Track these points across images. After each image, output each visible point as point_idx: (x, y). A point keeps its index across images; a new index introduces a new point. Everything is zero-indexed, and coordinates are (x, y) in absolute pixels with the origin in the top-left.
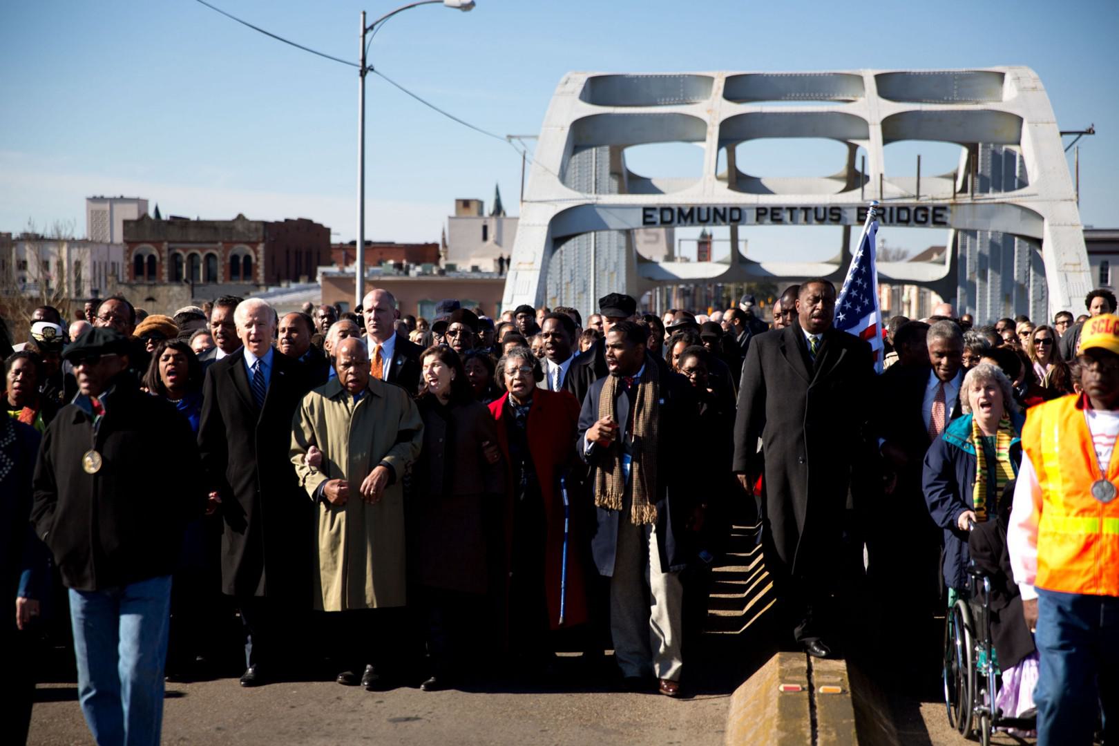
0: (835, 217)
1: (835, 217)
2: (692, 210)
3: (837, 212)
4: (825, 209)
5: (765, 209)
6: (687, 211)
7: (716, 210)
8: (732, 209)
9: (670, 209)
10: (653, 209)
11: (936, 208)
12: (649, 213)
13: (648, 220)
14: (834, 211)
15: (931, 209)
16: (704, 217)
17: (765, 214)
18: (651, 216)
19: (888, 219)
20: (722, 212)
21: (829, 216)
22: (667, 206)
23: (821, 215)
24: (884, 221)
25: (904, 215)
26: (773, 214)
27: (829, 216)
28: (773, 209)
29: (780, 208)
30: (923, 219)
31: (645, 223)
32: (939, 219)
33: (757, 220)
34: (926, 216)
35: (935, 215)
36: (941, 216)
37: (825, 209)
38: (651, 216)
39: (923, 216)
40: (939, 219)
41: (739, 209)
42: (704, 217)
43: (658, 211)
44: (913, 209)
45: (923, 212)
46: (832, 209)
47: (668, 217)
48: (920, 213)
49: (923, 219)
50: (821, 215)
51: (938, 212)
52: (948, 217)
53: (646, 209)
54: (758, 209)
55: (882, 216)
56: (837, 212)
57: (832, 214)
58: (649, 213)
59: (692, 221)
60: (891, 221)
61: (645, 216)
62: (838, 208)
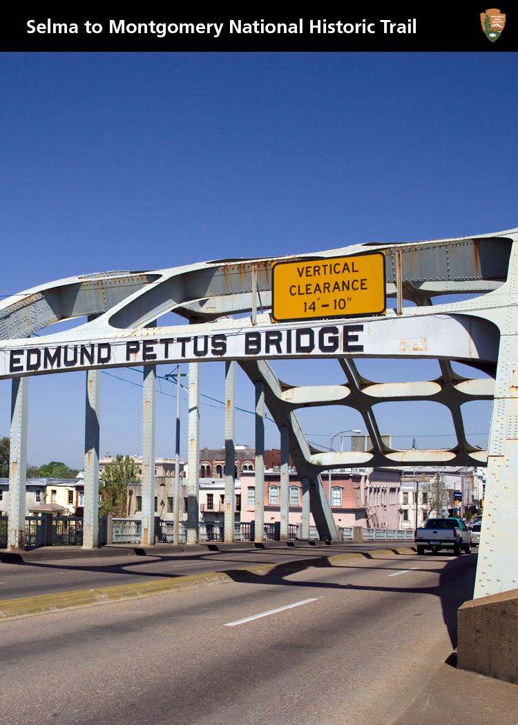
2: (59, 349)
3: (221, 341)
5: (136, 343)
6: (52, 353)
7: (83, 349)
8: (101, 346)
9: (37, 351)
10: (20, 352)
12: (15, 357)
13: (15, 365)
15: (341, 329)
16: (71, 357)
17: (136, 351)
18: (18, 361)
19: (283, 344)
20: (89, 350)
21: (210, 347)
22: (34, 347)
23: (201, 348)
24: (279, 350)
26: (145, 349)
27: (210, 347)
28: (145, 342)
30: (332, 344)
31: (12, 369)
32: (351, 344)
33: (128, 358)
34: (334, 340)
35: (347, 338)
36: (355, 338)
37: (206, 337)
38: (18, 361)
39: (331, 339)
40: (351, 344)
41: (107, 346)
42: (70, 358)
43: (26, 352)
45: (331, 335)
48: (326, 336)
49: (332, 344)
50: (201, 348)
53: (13, 352)
54: (129, 343)
55: (277, 343)
56: (221, 341)
57: (214, 344)
58: (15, 357)
59: (59, 365)
60: (289, 350)
61: (13, 361)
62: (223, 337)
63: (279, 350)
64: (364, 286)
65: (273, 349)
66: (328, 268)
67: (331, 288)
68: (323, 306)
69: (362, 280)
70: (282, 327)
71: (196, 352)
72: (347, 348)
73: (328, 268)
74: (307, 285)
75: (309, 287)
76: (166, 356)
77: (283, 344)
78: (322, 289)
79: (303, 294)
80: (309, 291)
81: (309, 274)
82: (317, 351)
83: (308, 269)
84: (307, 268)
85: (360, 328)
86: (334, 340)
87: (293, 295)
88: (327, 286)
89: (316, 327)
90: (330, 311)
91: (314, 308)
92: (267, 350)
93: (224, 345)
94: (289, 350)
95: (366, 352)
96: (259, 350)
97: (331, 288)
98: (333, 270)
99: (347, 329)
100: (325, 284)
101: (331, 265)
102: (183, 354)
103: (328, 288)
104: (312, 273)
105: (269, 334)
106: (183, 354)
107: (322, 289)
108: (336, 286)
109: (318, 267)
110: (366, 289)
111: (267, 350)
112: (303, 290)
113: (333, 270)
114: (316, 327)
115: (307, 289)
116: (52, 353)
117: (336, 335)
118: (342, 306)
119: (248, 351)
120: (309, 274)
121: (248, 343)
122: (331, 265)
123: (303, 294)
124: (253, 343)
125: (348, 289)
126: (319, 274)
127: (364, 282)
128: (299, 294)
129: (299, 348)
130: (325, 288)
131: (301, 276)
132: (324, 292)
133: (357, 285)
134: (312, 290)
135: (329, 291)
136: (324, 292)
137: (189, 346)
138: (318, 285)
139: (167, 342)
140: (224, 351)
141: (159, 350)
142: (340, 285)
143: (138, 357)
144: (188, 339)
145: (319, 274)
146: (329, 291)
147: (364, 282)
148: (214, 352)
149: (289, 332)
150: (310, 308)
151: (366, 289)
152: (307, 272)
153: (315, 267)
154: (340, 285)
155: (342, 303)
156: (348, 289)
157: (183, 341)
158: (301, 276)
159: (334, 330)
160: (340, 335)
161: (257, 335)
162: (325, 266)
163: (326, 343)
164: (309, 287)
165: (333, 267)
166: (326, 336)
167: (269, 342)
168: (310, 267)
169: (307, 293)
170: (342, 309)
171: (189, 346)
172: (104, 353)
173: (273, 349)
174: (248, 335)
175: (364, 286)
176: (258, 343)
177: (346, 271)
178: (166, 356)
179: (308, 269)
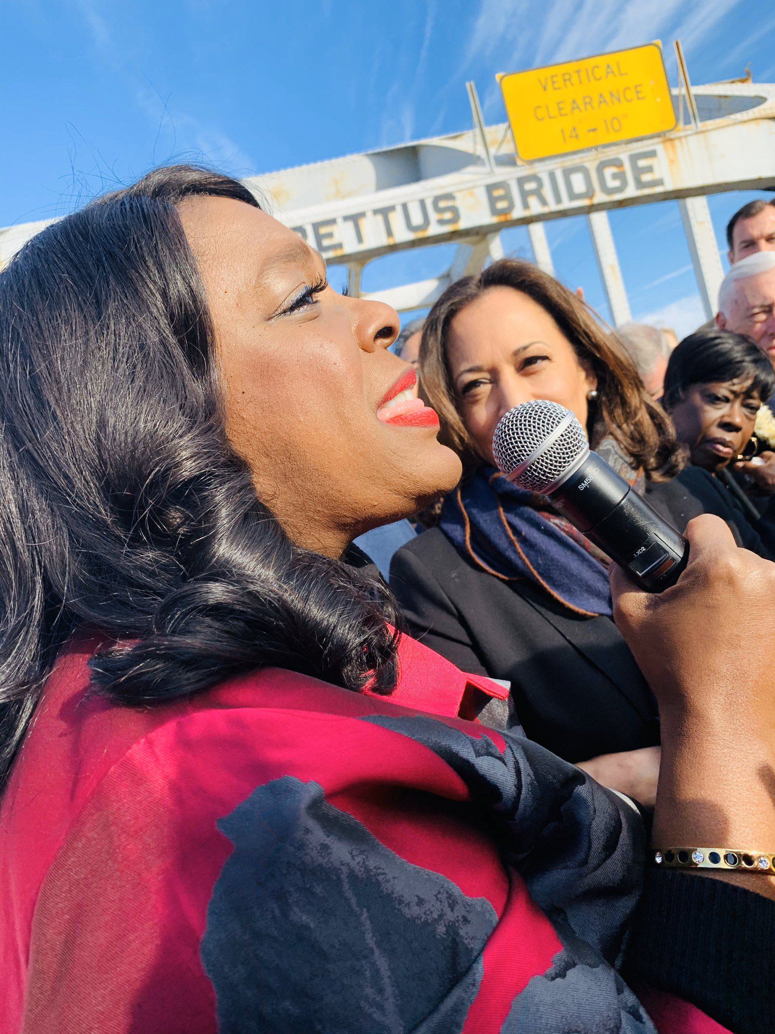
0: (448, 216)
1: (448, 216)
3: (449, 203)
4: (422, 203)
11: (634, 158)
14: (442, 204)
15: (625, 158)
19: (547, 192)
21: (433, 216)
23: (417, 219)
24: (544, 202)
29: (332, 222)
30: (616, 183)
32: (646, 178)
34: (620, 176)
35: (638, 172)
36: (650, 169)
39: (615, 176)
40: (646, 178)
44: (592, 167)
46: (437, 199)
48: (609, 172)
49: (616, 183)
50: (417, 219)
51: (642, 163)
55: (538, 193)
56: (449, 203)
60: (558, 200)
62: (449, 197)
63: (544, 202)
64: (640, 95)
65: (533, 201)
66: (583, 74)
67: (595, 103)
68: (589, 131)
69: (636, 87)
70: (542, 170)
71: (410, 227)
72: (640, 184)
73: (583, 74)
74: (558, 104)
75: (561, 105)
76: (360, 239)
77: (547, 192)
78: (582, 107)
79: (555, 117)
80: (563, 112)
81: (556, 86)
83: (555, 79)
84: (552, 77)
85: (652, 154)
86: (620, 176)
87: (539, 120)
88: (588, 100)
89: (591, 162)
90: (604, 137)
91: (577, 136)
92: (526, 206)
93: (454, 210)
94: (558, 200)
95: (669, 186)
96: (511, 207)
97: (595, 103)
98: (592, 78)
99: (634, 158)
100: (584, 98)
101: (587, 70)
102: (390, 233)
103: (590, 103)
104: (560, 83)
105: (521, 181)
106: (390, 233)
107: (582, 107)
108: (602, 100)
109: (567, 74)
110: (643, 98)
111: (526, 206)
112: (554, 111)
113: (592, 78)
114: (591, 162)
115: (560, 109)
117: (621, 169)
118: (616, 126)
119: (494, 211)
120: (556, 86)
121: (492, 201)
122: (587, 70)
123: (555, 117)
124: (501, 198)
125: (619, 100)
126: (572, 84)
127: (639, 89)
128: (551, 117)
129: (573, 196)
130: (586, 104)
131: (545, 89)
132: (586, 109)
133: (631, 94)
134: (567, 108)
135: (593, 108)
136: (586, 109)
137: (397, 219)
138: (574, 102)
139: (355, 219)
140: (455, 219)
142: (608, 98)
144: (392, 208)
145: (572, 84)
146: (593, 108)
147: (639, 89)
148: (441, 222)
150: (571, 137)
151: (643, 98)
152: (553, 83)
153: (564, 75)
154: (608, 98)
155: (615, 121)
156: (619, 100)
157: (384, 212)
158: (545, 89)
159: (617, 163)
162: (578, 72)
164: (561, 105)
165: (590, 74)
166: (609, 172)
167: (525, 195)
168: (556, 76)
169: (562, 115)
170: (616, 131)
171: (397, 219)
173: (533, 201)
174: (490, 188)
175: (640, 95)
176: (507, 197)
177: (610, 75)
178: (360, 239)
179: (555, 79)
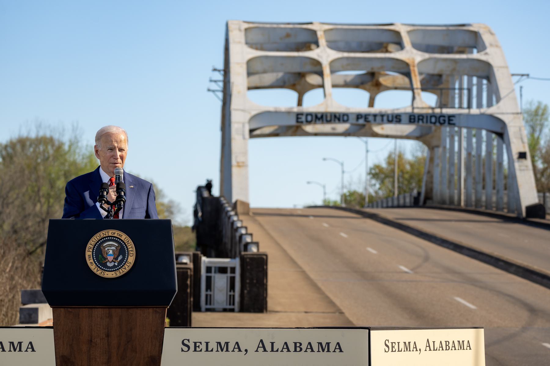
6: (319, 116)
16: (329, 119)
19: (425, 120)
21: (395, 119)
25: (433, 120)
27: (395, 119)
34: (444, 121)
35: (449, 120)
42: (329, 119)
47: (309, 118)
50: (390, 119)
52: (455, 121)
55: (422, 120)
59: (323, 121)
60: (427, 122)
61: (298, 118)
77: (425, 120)
82: (438, 124)
86: (444, 121)
116: (319, 116)
121: (410, 119)
137: (385, 118)
141: (371, 118)
143: (361, 121)
149: (427, 117)
160: (447, 119)
161: (414, 116)
163: (442, 121)
167: (419, 119)
171: (385, 118)
172: (345, 118)
176: (414, 119)
